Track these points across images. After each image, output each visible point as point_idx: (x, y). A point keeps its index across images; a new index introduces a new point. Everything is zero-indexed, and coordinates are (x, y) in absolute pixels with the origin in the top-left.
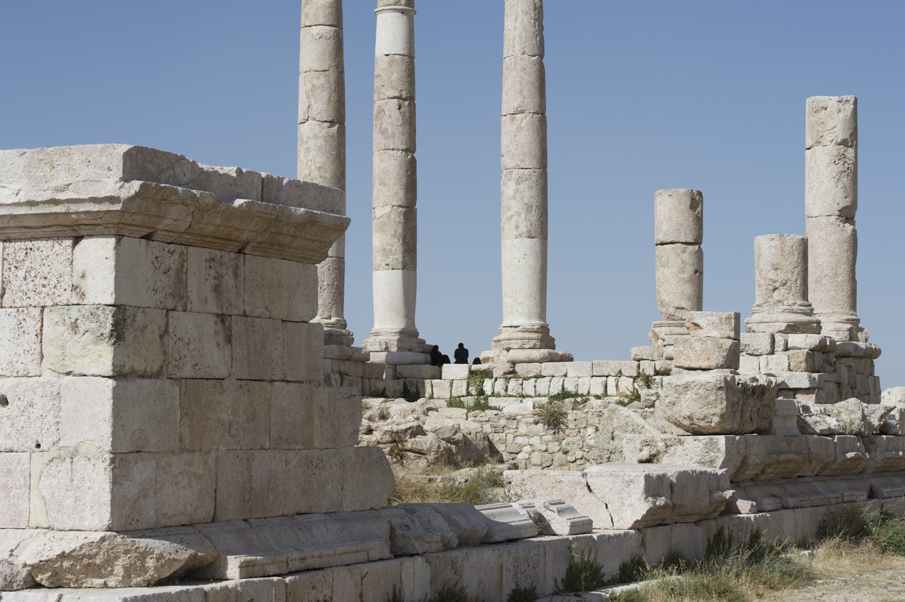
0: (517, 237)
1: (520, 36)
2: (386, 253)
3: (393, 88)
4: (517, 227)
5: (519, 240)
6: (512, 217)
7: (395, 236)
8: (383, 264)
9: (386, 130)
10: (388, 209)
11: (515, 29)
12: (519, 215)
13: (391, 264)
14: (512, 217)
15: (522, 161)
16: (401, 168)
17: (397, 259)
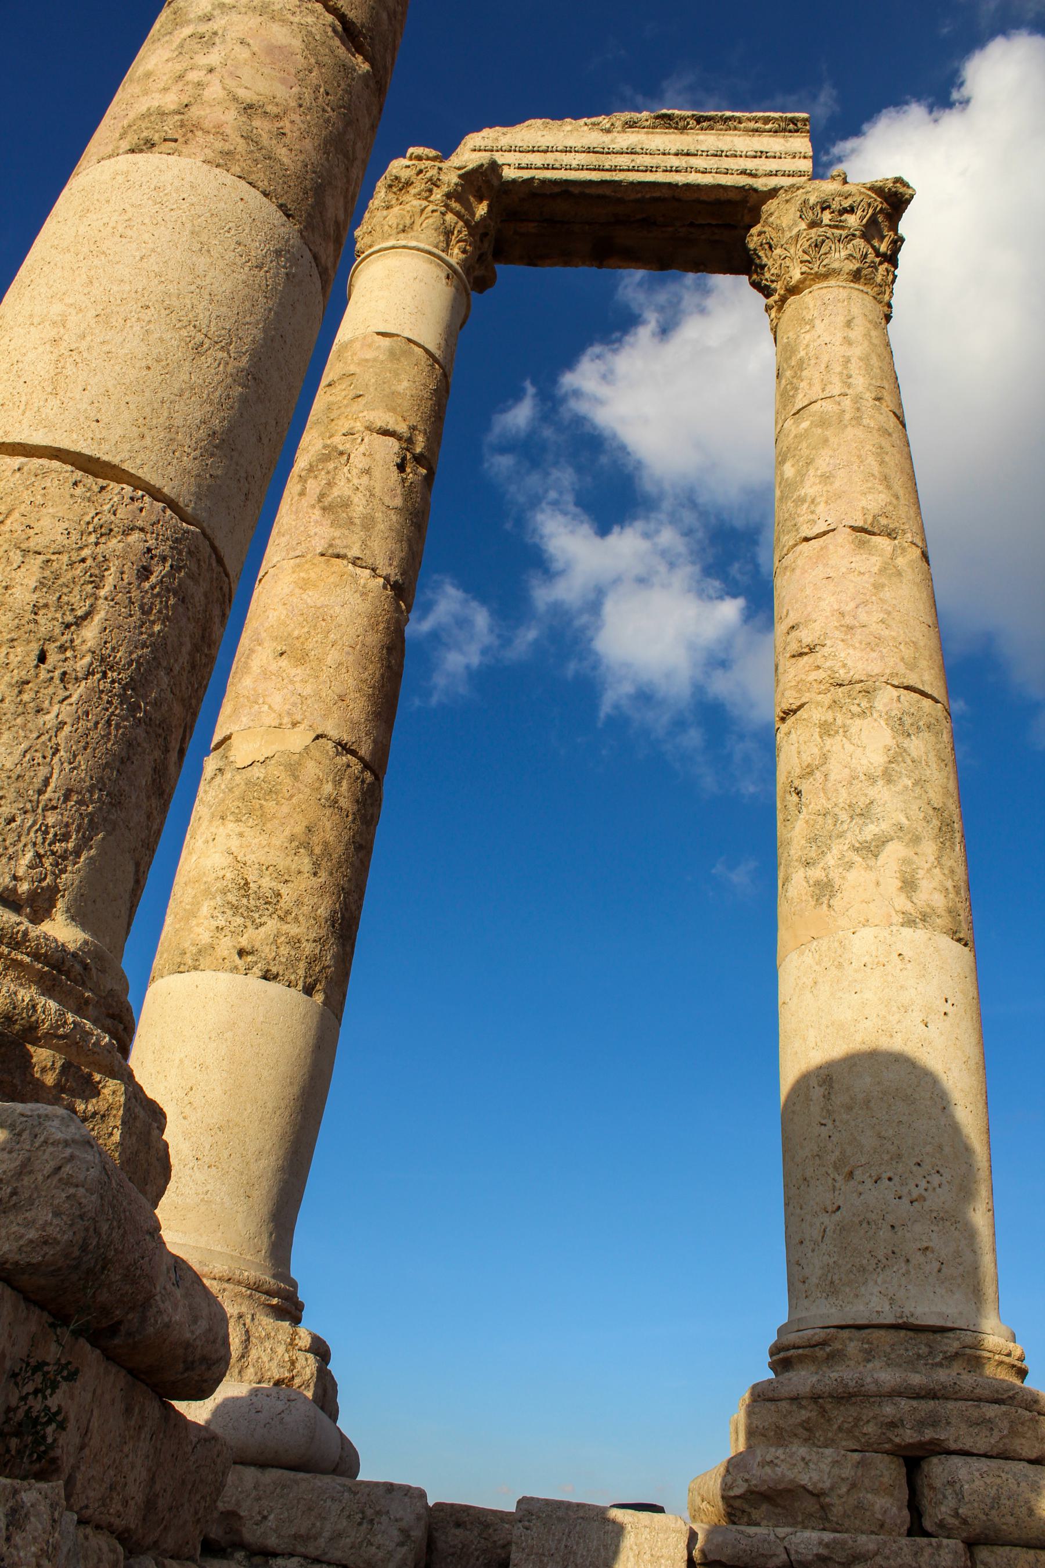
0: (909, 922)
1: (865, 359)
2: (246, 899)
3: (393, 410)
4: (909, 885)
5: (919, 935)
6: (883, 841)
7: (307, 845)
8: (226, 946)
9: (346, 504)
10: (298, 740)
11: (848, 342)
12: (916, 840)
13: (268, 952)
14: (883, 841)
15: (912, 666)
16: (374, 626)
17: (295, 942)
